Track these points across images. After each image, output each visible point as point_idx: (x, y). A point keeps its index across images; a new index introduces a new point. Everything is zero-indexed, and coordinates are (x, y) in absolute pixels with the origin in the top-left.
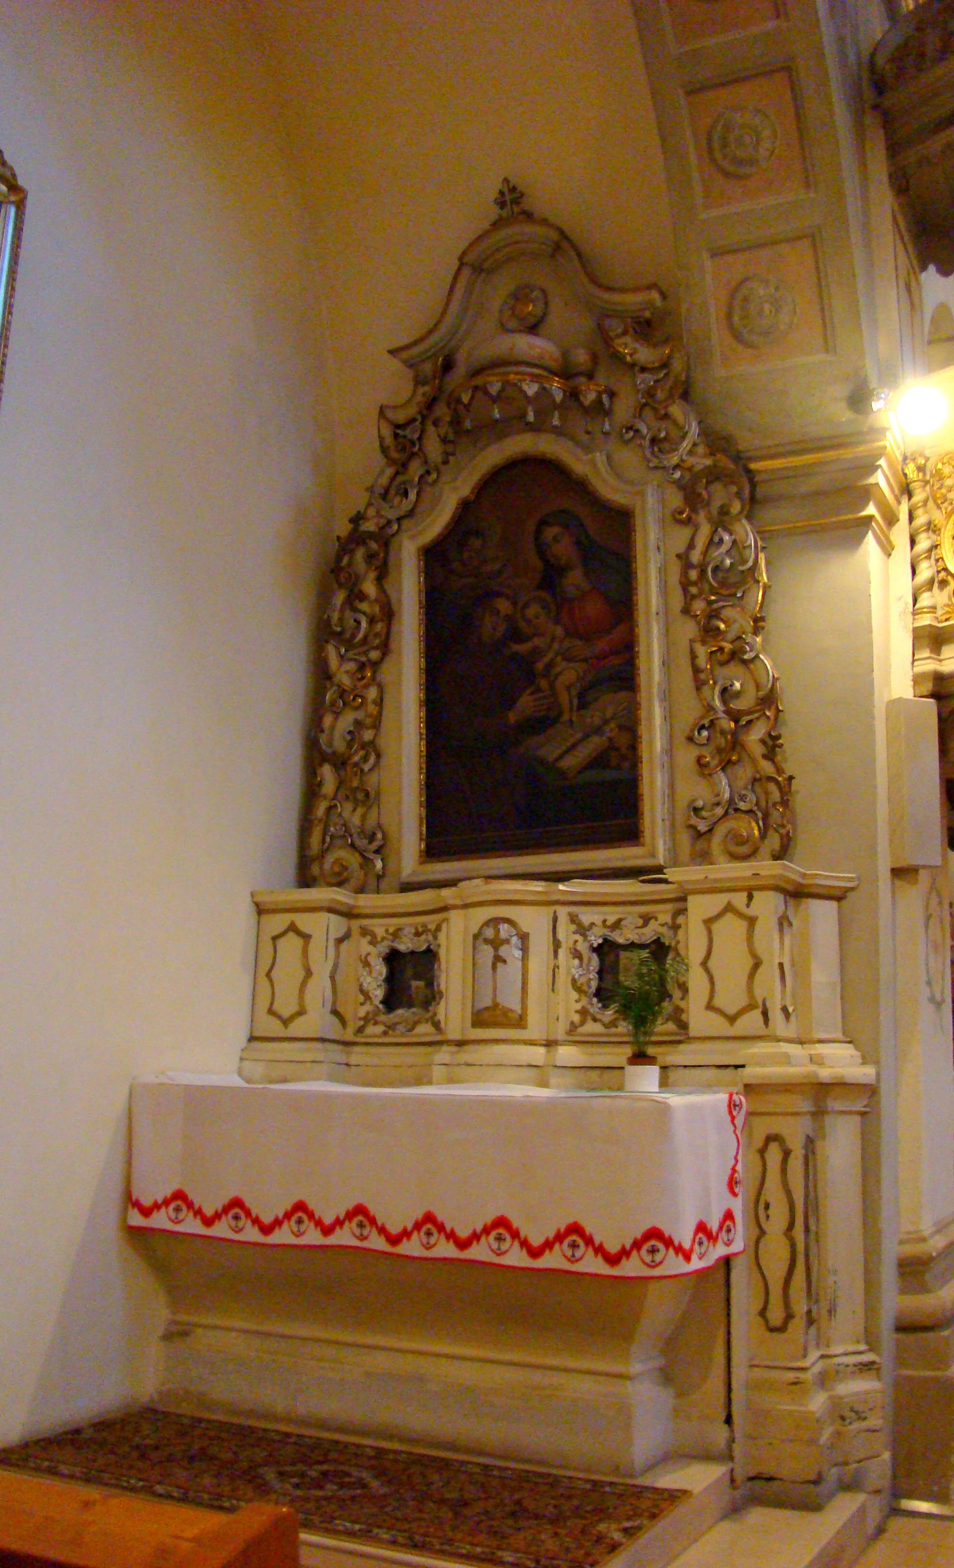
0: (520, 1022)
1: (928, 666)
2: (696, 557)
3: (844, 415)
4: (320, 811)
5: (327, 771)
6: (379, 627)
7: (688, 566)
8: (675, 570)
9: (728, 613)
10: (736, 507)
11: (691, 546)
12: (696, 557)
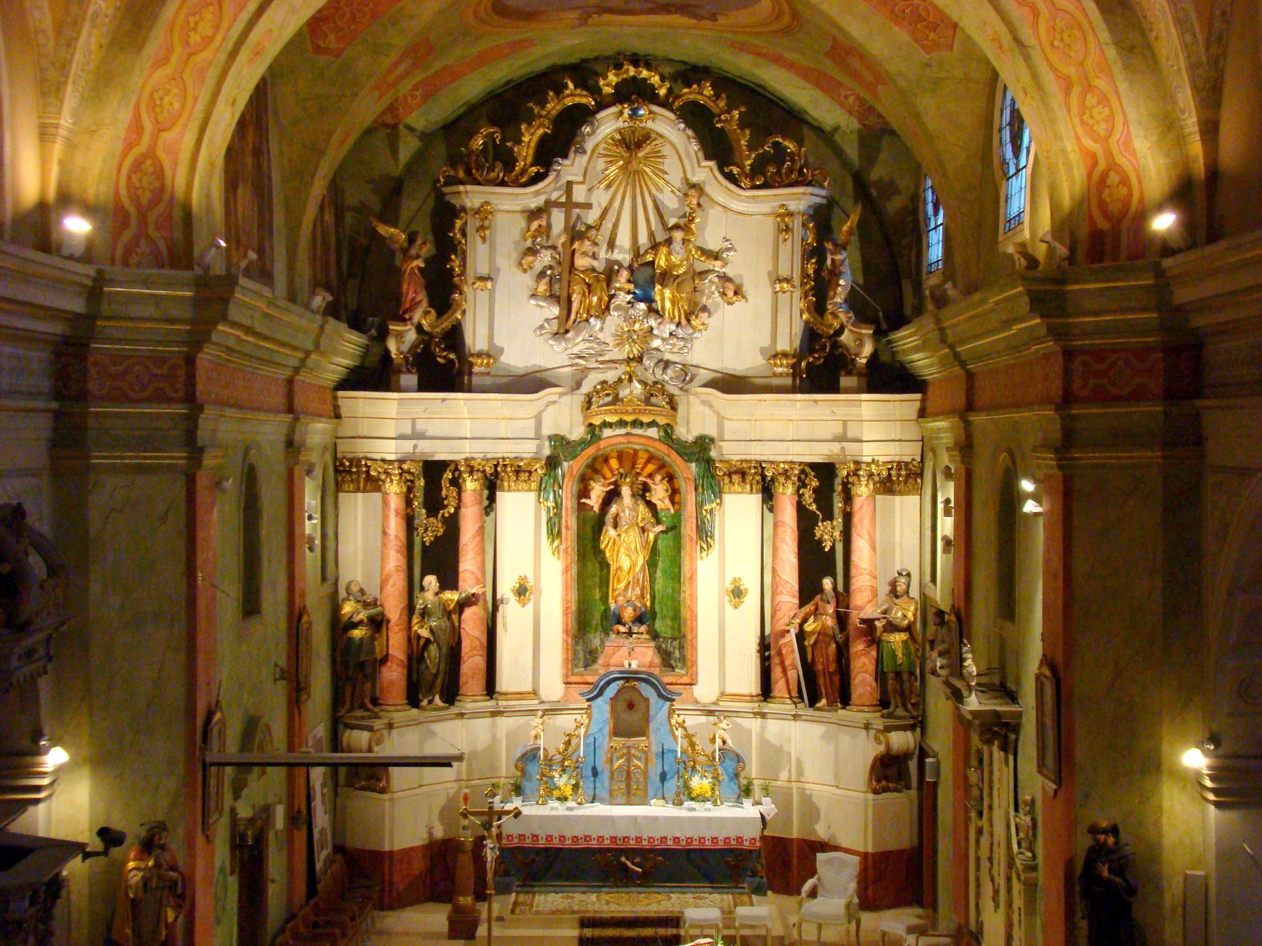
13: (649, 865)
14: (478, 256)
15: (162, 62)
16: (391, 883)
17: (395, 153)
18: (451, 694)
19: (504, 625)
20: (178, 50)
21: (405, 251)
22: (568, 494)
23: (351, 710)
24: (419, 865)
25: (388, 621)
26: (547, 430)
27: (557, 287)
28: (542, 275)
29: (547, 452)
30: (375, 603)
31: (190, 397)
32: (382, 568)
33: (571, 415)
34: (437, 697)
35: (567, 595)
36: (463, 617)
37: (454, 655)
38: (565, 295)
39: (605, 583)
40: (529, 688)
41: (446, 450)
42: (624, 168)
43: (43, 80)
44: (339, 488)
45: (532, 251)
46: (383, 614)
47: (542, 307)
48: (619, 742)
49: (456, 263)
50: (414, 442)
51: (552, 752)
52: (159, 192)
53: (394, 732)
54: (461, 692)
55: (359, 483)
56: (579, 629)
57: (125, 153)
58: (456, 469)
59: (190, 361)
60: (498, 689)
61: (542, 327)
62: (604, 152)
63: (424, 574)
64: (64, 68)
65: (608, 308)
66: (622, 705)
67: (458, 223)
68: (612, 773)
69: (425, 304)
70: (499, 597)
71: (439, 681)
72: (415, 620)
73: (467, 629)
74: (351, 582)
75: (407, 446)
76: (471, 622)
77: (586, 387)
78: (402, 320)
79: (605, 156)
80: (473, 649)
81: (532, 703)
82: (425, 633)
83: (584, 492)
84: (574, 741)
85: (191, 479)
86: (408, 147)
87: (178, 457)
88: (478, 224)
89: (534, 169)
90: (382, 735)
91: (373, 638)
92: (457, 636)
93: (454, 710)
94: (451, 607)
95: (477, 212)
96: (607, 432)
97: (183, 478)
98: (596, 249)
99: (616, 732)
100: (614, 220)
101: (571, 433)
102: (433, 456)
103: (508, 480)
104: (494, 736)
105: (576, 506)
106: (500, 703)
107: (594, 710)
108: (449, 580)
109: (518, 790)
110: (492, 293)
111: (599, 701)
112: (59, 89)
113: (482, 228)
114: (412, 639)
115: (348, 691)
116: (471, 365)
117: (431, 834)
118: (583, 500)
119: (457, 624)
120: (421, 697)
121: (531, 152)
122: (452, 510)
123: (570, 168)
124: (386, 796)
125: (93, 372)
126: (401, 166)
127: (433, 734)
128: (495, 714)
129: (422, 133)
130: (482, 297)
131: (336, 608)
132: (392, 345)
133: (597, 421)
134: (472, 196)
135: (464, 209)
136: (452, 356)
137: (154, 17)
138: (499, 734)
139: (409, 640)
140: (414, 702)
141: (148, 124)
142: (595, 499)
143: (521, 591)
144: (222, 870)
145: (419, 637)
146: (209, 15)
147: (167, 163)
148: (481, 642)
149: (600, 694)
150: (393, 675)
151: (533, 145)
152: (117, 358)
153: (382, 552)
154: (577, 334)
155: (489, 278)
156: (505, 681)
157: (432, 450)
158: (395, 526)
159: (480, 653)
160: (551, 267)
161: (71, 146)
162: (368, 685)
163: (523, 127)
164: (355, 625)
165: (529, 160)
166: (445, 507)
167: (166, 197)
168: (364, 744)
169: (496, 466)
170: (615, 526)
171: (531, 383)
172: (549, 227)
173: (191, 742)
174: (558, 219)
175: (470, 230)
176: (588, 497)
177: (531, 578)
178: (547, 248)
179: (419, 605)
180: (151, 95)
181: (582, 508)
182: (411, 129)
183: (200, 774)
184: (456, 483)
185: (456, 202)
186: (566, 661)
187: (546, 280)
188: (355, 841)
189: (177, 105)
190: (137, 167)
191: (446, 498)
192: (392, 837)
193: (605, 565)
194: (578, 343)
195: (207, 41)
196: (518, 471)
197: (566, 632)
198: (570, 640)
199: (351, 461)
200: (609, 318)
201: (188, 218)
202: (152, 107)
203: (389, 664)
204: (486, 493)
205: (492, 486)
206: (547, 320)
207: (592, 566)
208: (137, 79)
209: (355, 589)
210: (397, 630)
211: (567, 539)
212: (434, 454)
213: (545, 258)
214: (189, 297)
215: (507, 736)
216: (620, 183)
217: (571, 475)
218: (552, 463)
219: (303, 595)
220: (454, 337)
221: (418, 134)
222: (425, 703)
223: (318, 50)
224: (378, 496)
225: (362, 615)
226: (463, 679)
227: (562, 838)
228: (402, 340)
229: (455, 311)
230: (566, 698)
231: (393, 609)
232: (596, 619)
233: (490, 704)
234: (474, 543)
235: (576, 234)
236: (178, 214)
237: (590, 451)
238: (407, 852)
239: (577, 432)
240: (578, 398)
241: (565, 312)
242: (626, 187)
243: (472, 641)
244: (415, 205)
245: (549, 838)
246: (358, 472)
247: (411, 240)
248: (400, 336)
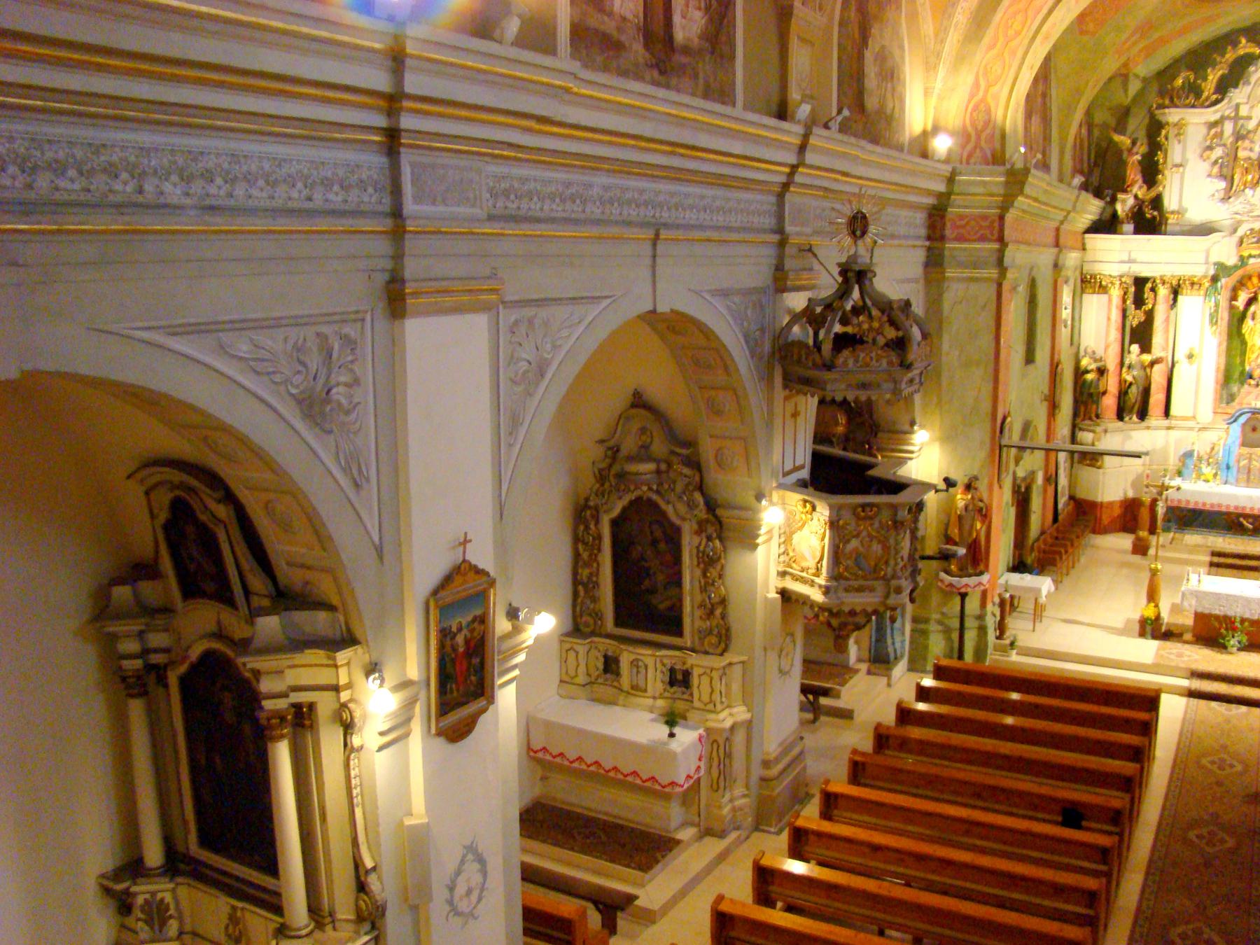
0: (645, 691)
1: (781, 585)
2: (702, 548)
3: (752, 500)
4: (579, 600)
5: (580, 588)
6: (597, 542)
7: (698, 551)
8: (695, 551)
9: (711, 570)
10: (715, 535)
11: (700, 544)
12: (702, 548)
13: (1257, 524)
14: (1175, 151)
15: (992, 46)
16: (1100, 519)
17: (1126, 91)
18: (1143, 414)
20: (1001, 40)
21: (1130, 151)
22: (1223, 299)
23: (1083, 420)
24: (1117, 511)
26: (1213, 259)
27: (1225, 170)
28: (1215, 162)
29: (1212, 272)
30: (1101, 360)
31: (1001, 239)
32: (1106, 340)
34: (1135, 418)
37: (1146, 392)
38: (1230, 174)
39: (1243, 353)
40: (1190, 414)
43: (927, 63)
44: (1083, 291)
45: (1210, 148)
46: (1105, 366)
48: (1245, 450)
49: (1160, 157)
50: (1129, 265)
51: (1202, 453)
52: (987, 123)
53: (1108, 435)
57: (969, 102)
58: (1154, 281)
59: (1001, 218)
61: (1213, 195)
63: (1131, 343)
64: (938, 55)
66: (1248, 428)
67: (1164, 132)
68: (1239, 469)
69: (1140, 182)
70: (1175, 359)
72: (1124, 370)
75: (1124, 268)
76: (1158, 375)
77: (1240, 232)
78: (1125, 191)
81: (1191, 424)
82: (1129, 378)
83: (1234, 298)
84: (1216, 449)
85: (1000, 285)
86: (1134, 87)
87: (993, 273)
88: (1176, 132)
89: (1214, 97)
91: (1099, 379)
93: (1144, 424)
95: (1176, 125)
96: (1252, 261)
97: (995, 286)
98: (1252, 145)
99: (1244, 444)
103: (1186, 290)
104: (1167, 442)
107: (1231, 431)
108: (1146, 348)
109: (1179, 473)
111: (1235, 424)
112: (935, 67)
113: (1178, 134)
114: (1121, 382)
115: (1082, 409)
116: (1167, 219)
117: (1125, 494)
121: (1214, 85)
123: (1238, 95)
124: (1101, 471)
125: (948, 225)
126: (1129, 99)
127: (1130, 438)
128: (1169, 428)
131: (1078, 362)
132: (1119, 207)
133: (1246, 254)
134: (1172, 115)
135: (1167, 123)
136: (1155, 213)
137: (989, 23)
140: (1120, 417)
141: (982, 83)
142: (1240, 303)
143: (1190, 356)
144: (1007, 503)
145: (1125, 381)
146: (1019, 17)
147: (992, 105)
149: (1235, 421)
150: (1109, 402)
151: (1215, 81)
152: (961, 217)
154: (1236, 199)
155: (1181, 165)
156: (1174, 410)
158: (1116, 315)
160: (1222, 158)
161: (940, 98)
162: (1094, 406)
163: (1209, 70)
164: (1087, 372)
165: (1212, 91)
166: (1144, 304)
167: (991, 125)
170: (1253, 319)
171: (1204, 230)
172: (1222, 132)
173: (994, 431)
174: (1228, 128)
175: (1171, 136)
178: (1220, 145)
179: (1127, 362)
180: (986, 66)
181: (1232, 307)
182: (1136, 76)
183: (997, 452)
184: (1153, 290)
185: (1163, 119)
186: (1215, 400)
187: (1218, 166)
188: (1082, 494)
189: (999, 71)
190: (976, 108)
192: (1103, 494)
193: (1244, 343)
194: (1237, 205)
195: (1018, 33)
196: (1193, 284)
197: (1217, 383)
201: (1003, 136)
202: (985, 74)
204: (1172, 296)
205: (1176, 292)
206: (1217, 191)
207: (1236, 343)
208: (978, 58)
209: (1089, 351)
213: (1218, 152)
214: (1001, 182)
218: (1215, 279)
219: (1060, 352)
220: (1157, 202)
222: (1127, 419)
223: (1082, 32)
224: (1104, 297)
225: (1093, 366)
227: (1204, 504)
228: (1125, 204)
230: (1213, 422)
231: (1112, 364)
232: (1236, 375)
233: (1166, 423)
235: (1239, 137)
236: (997, 137)
238: (1111, 504)
239: (1231, 260)
240: (1235, 238)
244: (1137, 123)
245: (1196, 503)
246: (1095, 282)
247: (1134, 143)
248: (1124, 201)
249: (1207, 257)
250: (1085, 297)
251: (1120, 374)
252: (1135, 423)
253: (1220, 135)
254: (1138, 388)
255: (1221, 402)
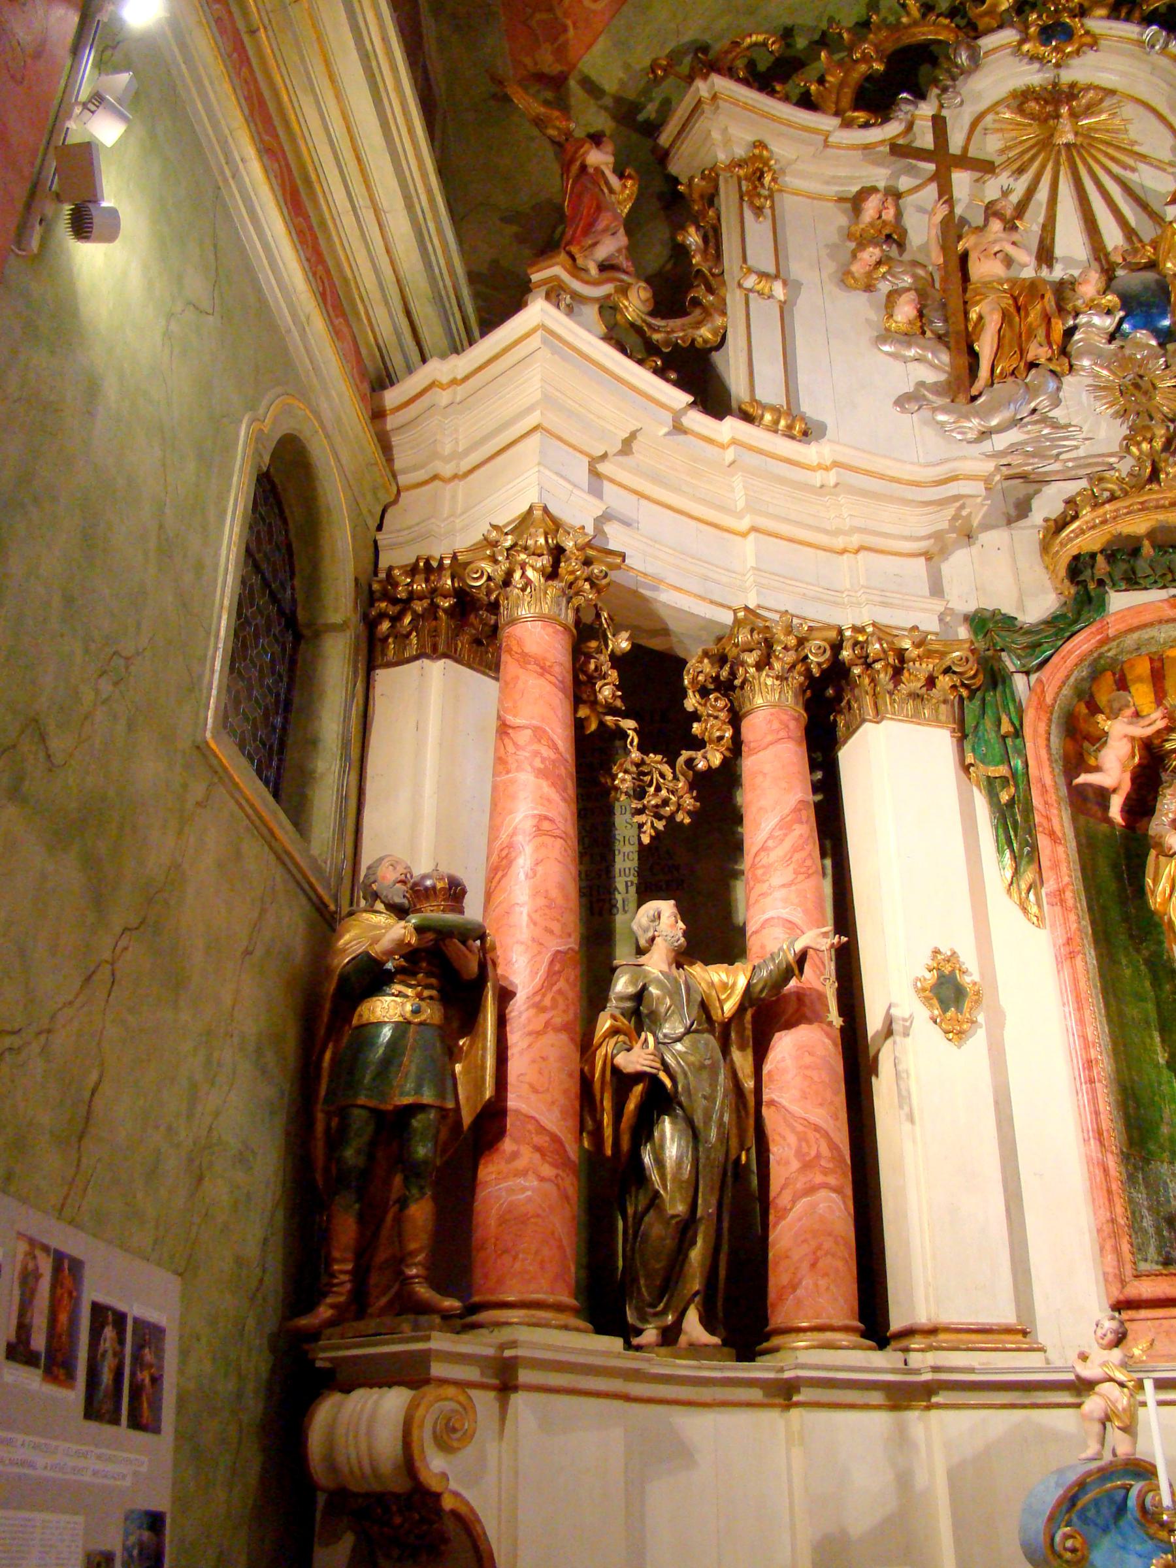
19: (903, 1098)
25: (505, 996)
32: (494, 830)
33: (1016, 572)
34: (692, 1319)
35: (1081, 1022)
36: (766, 1068)
41: (694, 586)
42: (1046, 143)
47: (906, 360)
54: (777, 1319)
55: (435, 633)
56: (1131, 1142)
60: (897, 1322)
62: (997, 126)
65: (1064, 352)
70: (874, 1024)
71: (696, 1254)
72: (605, 1023)
73: (785, 1103)
74: (381, 859)
79: (1001, 130)
80: (807, 1166)
90: (468, 1408)
91: (452, 1054)
92: (751, 1121)
93: (760, 1369)
94: (730, 1007)
96: (1119, 601)
100: (1041, 220)
101: (1021, 607)
102: (655, 588)
104: (904, 1481)
105: (1064, 791)
106: (915, 1359)
110: (785, 310)
118: (1083, 778)
119: (749, 1084)
120: (631, 1318)
122: (716, 760)
129: (618, 100)
130: (765, 315)
138: (921, 1480)
139: (586, 1082)
145: (623, 1081)
148: (833, 1146)
153: (495, 789)
157: (650, 570)
159: (832, 1180)
166: (698, 744)
168: (387, 1444)
169: (837, 647)
176: (1097, 769)
177: (969, 960)
179: (622, 985)
182: (591, 88)
186: (1109, 1233)
191: (695, 717)
198: (1112, 1162)
199: (413, 571)
200: (1068, 380)
203: (508, 1145)
206: (921, 384)
209: (388, 876)
210: (538, 1024)
211: (1055, 866)
212: (657, 583)
215: (955, 1477)
216: (1043, 167)
217: (1041, 704)
221: (608, 101)
222: (650, 1335)
226: (777, 1279)
229: (698, 324)
234: (788, 844)
237: (1082, 643)
241: (964, 360)
242: (1057, 164)
243: (802, 1138)
249: (937, 589)
250: (382, 676)
251: (586, 1046)
252: (696, 1351)
253: (894, 237)
254: (695, 1135)
255: (1139, 1250)
